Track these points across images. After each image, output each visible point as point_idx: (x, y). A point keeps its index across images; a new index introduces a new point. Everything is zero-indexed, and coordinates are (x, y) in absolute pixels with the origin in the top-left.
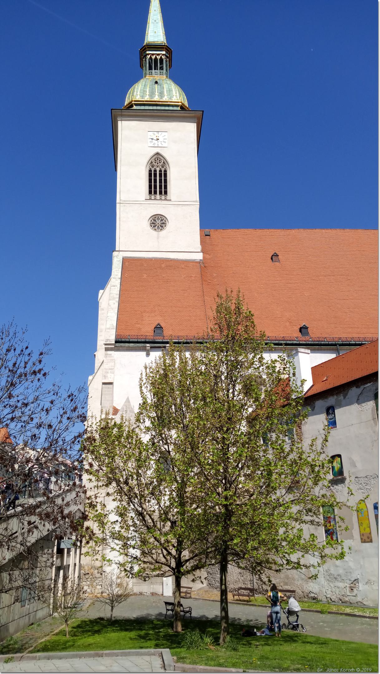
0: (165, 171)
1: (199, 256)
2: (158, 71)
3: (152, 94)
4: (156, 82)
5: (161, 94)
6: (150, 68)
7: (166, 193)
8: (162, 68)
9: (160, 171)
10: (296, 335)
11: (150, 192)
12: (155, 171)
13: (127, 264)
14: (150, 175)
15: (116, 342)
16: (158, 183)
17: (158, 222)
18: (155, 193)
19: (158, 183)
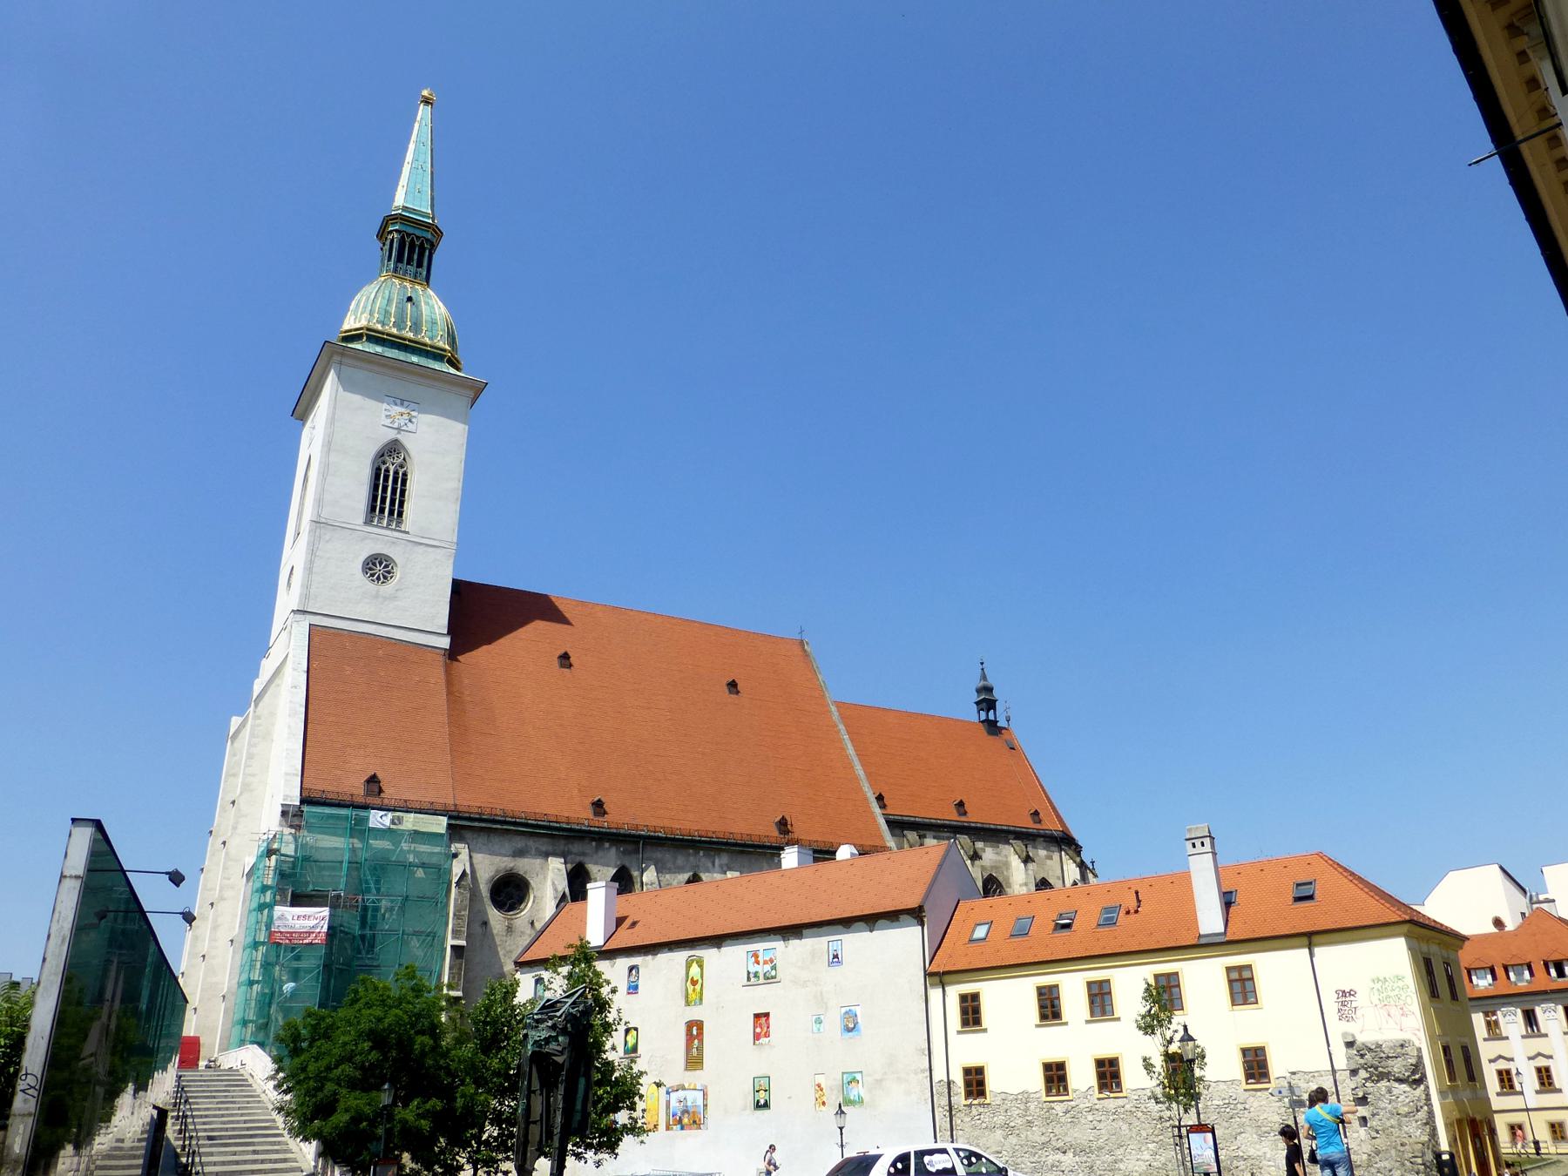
0: (405, 474)
1: (445, 642)
2: (411, 269)
3: (399, 324)
4: (410, 299)
5: (416, 327)
6: (400, 259)
7: (400, 514)
8: (420, 265)
9: (396, 473)
10: (584, 815)
11: (373, 509)
12: (387, 470)
13: (316, 639)
14: (377, 477)
15: (302, 802)
16: (387, 492)
17: (378, 567)
18: (382, 511)
19: (387, 492)
